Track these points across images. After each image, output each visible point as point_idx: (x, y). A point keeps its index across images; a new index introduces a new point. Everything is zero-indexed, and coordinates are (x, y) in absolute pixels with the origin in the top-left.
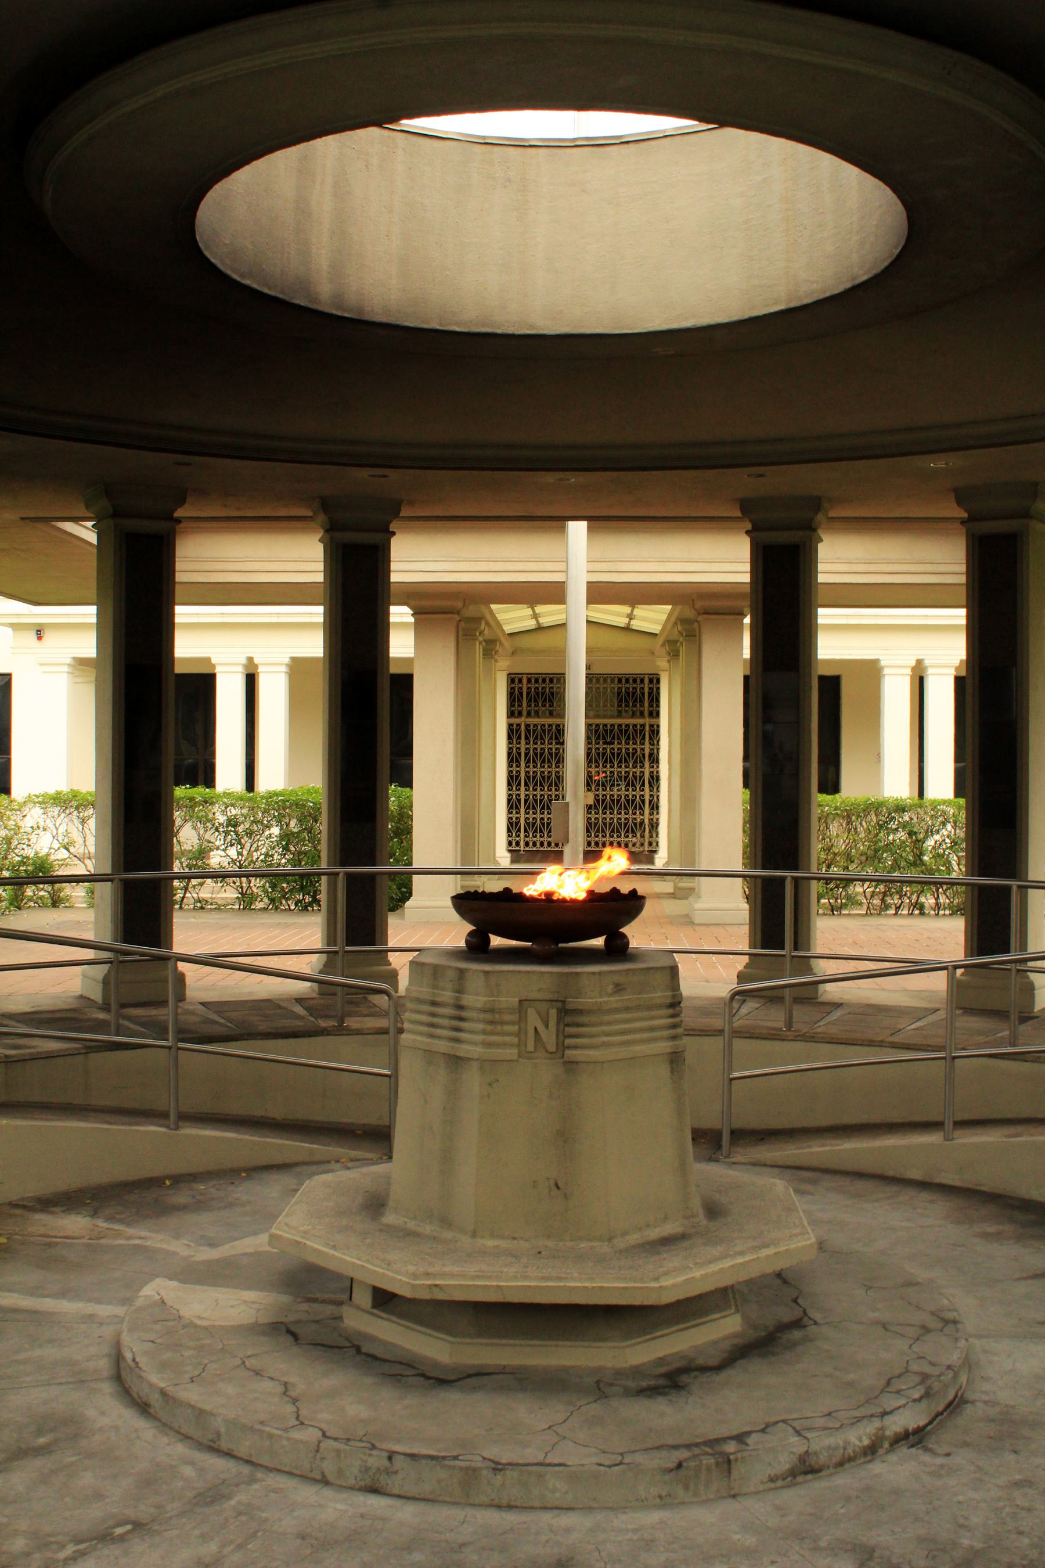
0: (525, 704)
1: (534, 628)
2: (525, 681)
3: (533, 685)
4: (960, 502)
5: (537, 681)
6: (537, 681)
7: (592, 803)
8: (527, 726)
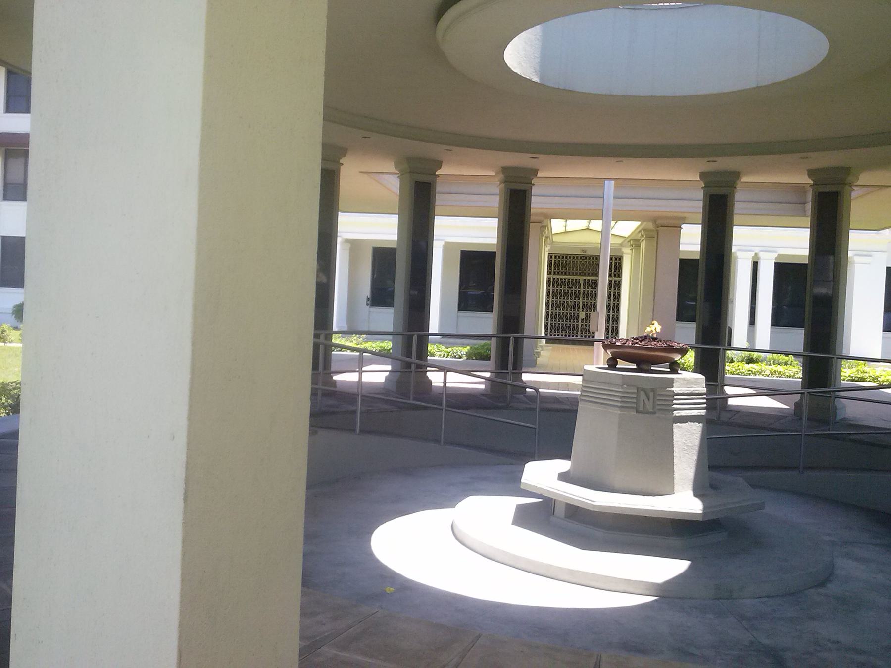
0: (553, 268)
1: (563, 231)
2: (553, 257)
3: (557, 260)
4: (809, 176)
5: (559, 257)
6: (559, 257)
7: (584, 317)
8: (554, 279)
